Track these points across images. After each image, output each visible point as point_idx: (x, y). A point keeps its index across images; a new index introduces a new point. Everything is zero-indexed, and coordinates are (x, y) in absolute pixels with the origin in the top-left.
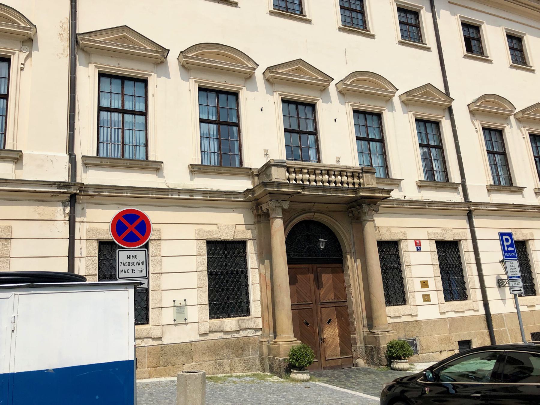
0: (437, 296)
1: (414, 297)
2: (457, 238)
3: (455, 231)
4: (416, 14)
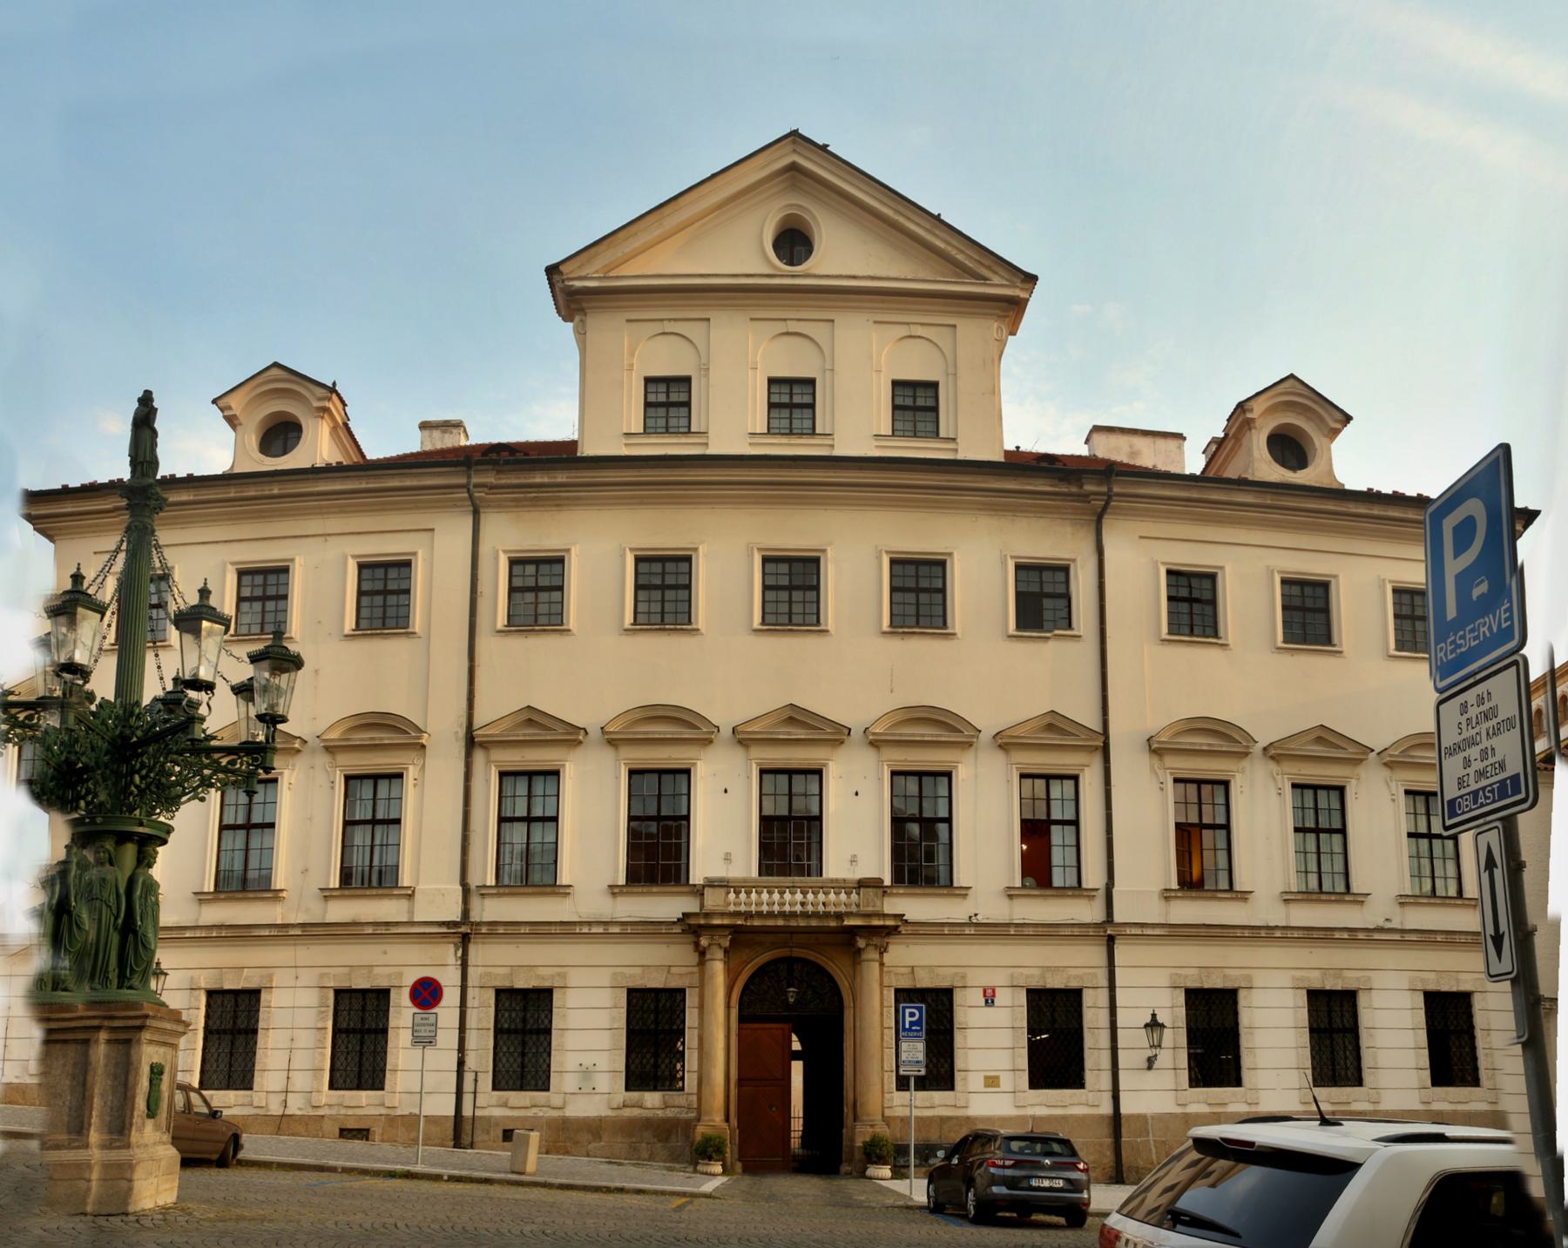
1: (965, 1079)
3: (1073, 972)
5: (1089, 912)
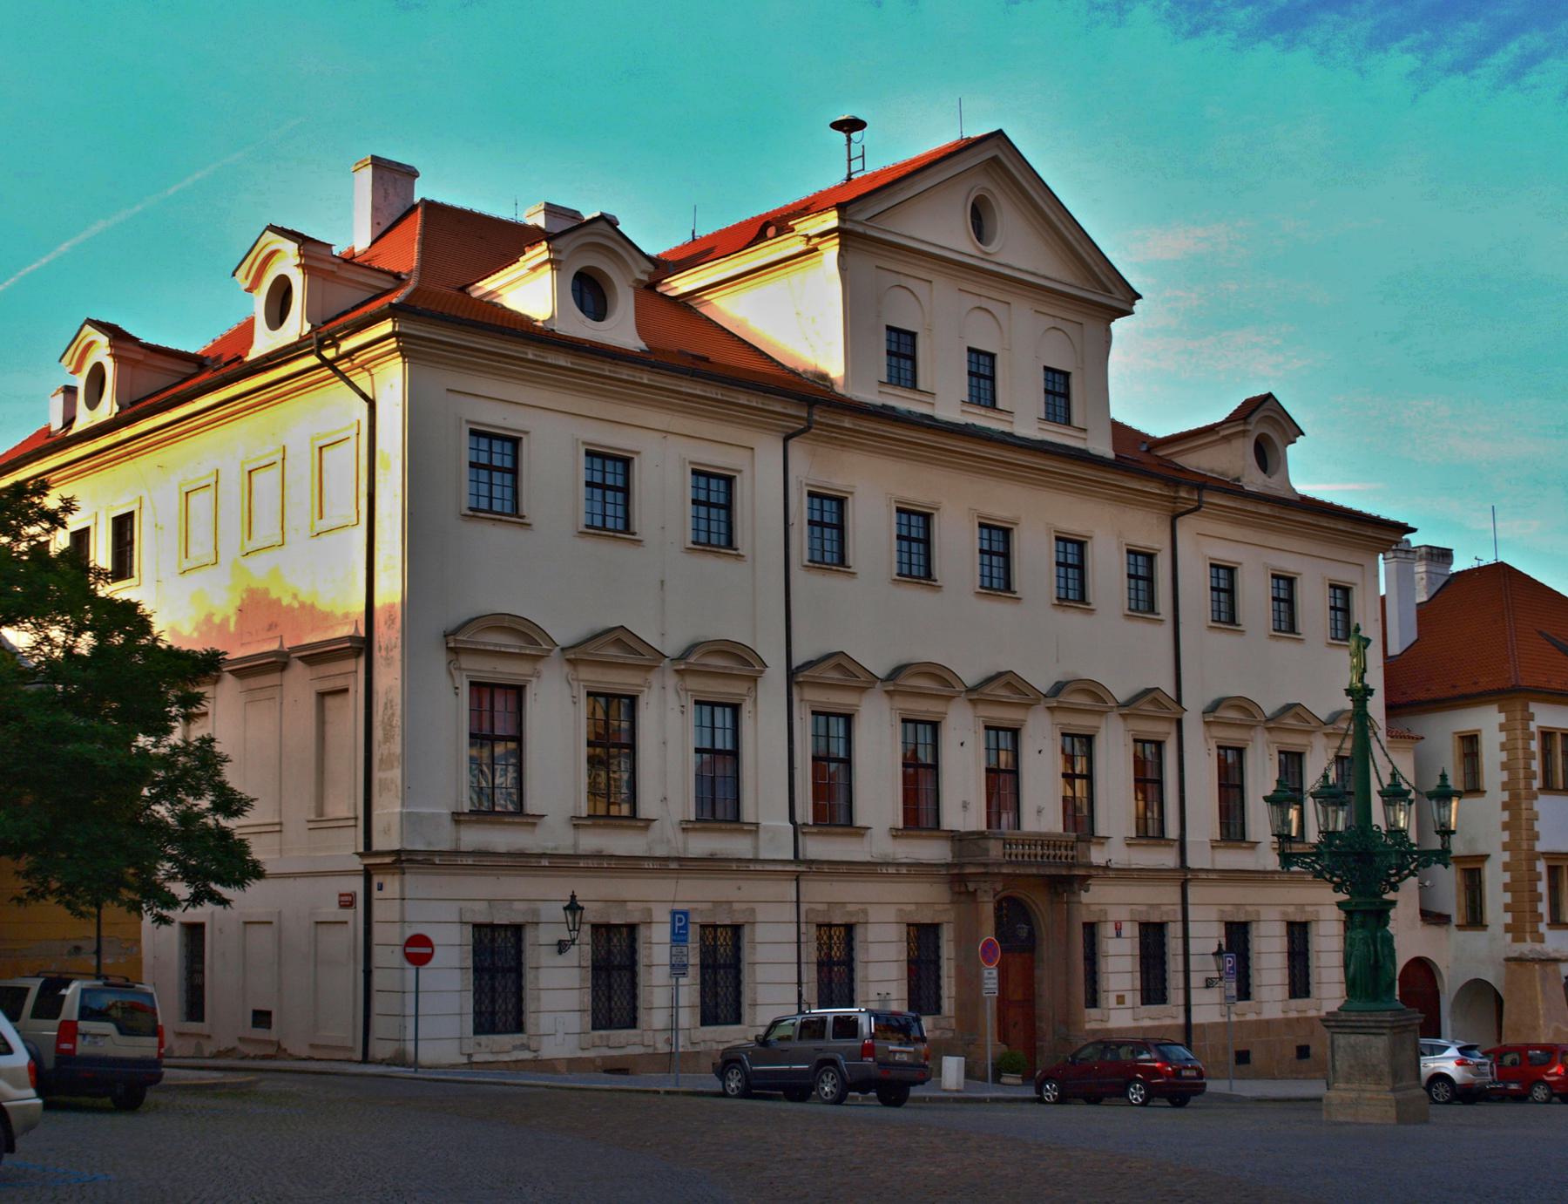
0: (1133, 998)
2: (1165, 919)
4: (1150, 557)
5: (1166, 858)
